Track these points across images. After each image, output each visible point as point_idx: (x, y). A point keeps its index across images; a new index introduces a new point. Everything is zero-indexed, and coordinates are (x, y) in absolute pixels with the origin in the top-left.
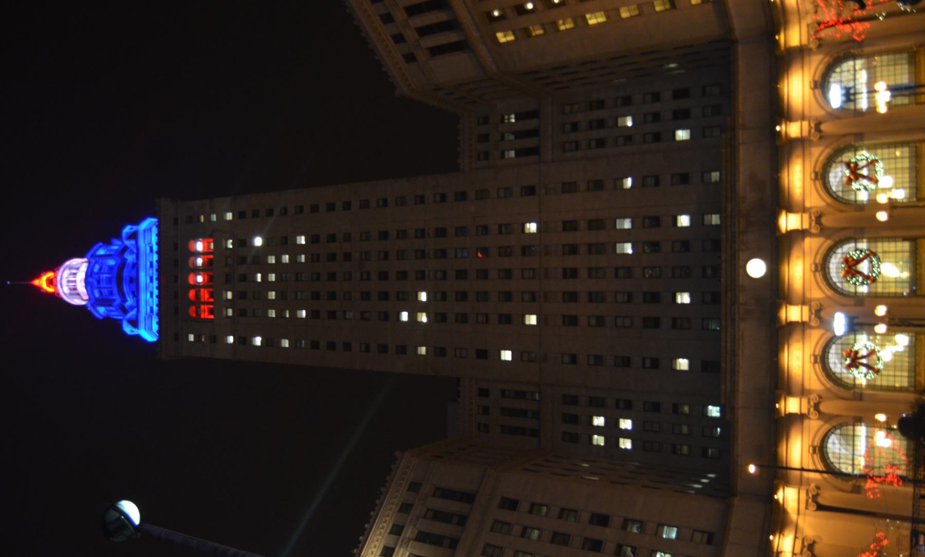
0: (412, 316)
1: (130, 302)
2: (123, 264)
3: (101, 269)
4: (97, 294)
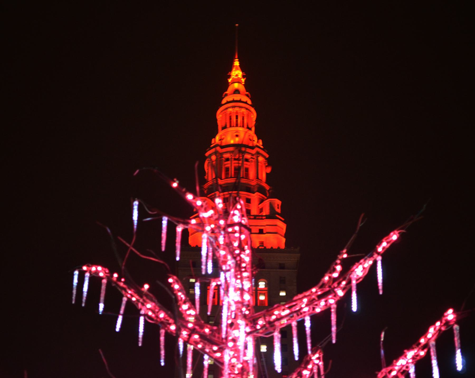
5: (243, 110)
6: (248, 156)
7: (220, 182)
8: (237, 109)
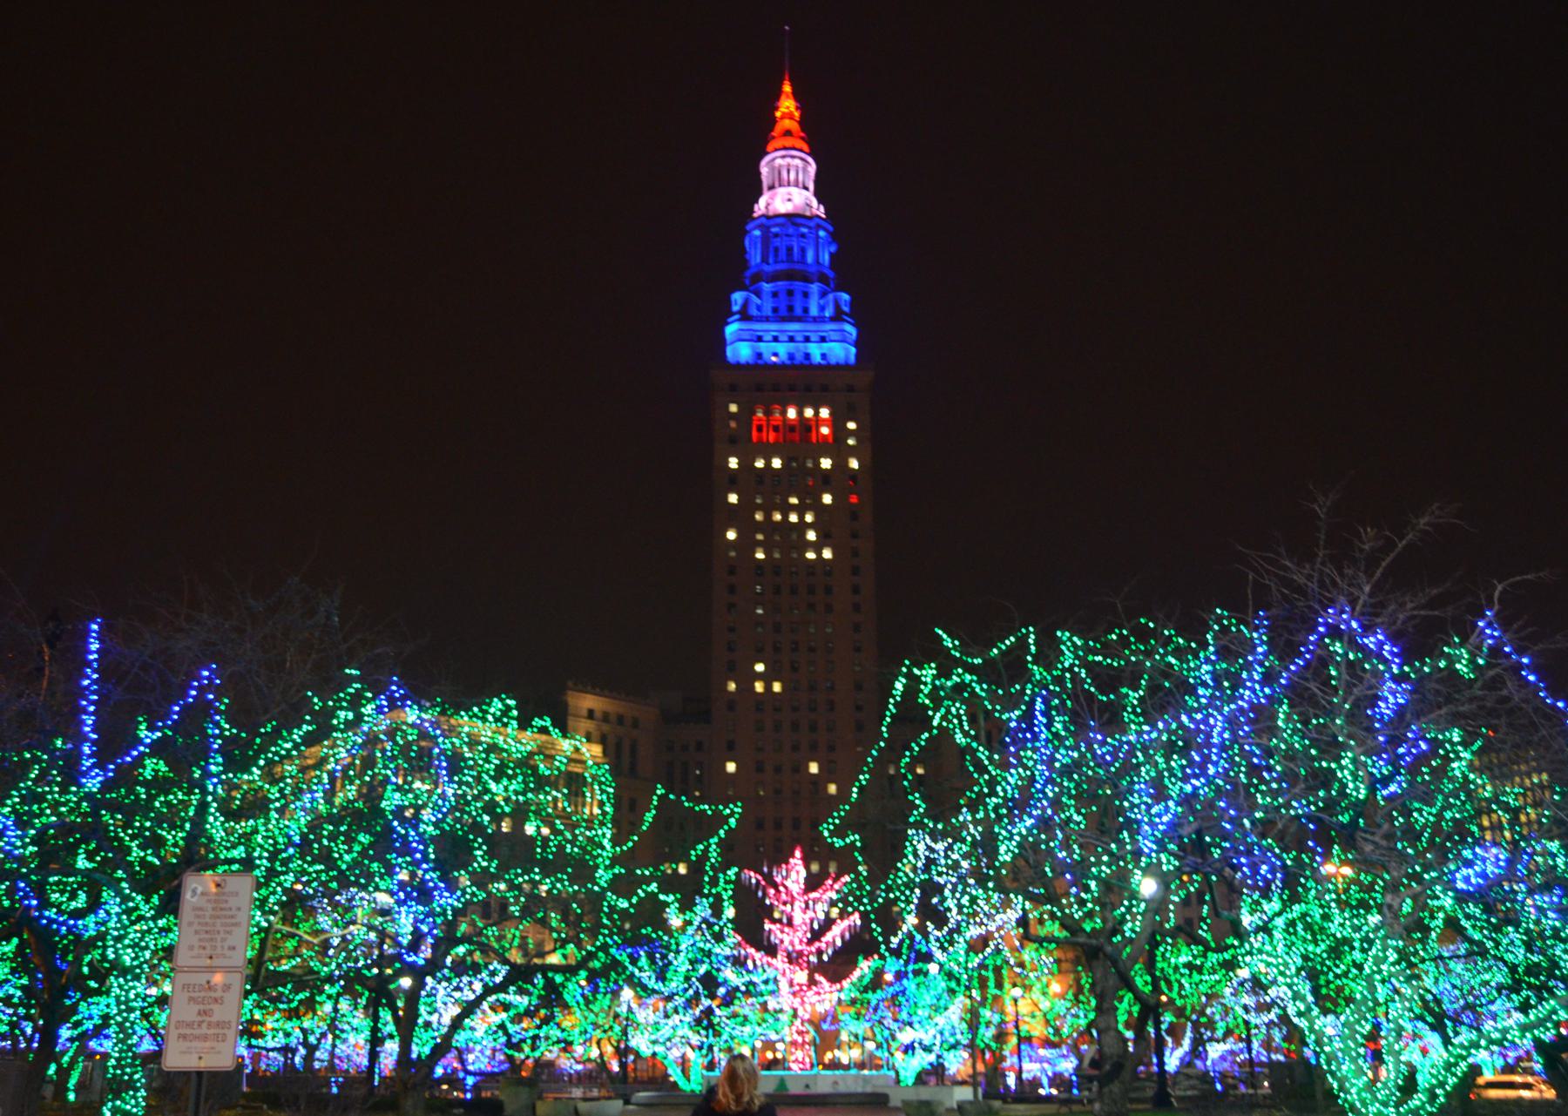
0: (759, 676)
1: (767, 287)
2: (807, 279)
3: (803, 235)
4: (775, 230)
5: (797, 162)
6: (805, 230)
7: (766, 268)
8: (789, 160)
